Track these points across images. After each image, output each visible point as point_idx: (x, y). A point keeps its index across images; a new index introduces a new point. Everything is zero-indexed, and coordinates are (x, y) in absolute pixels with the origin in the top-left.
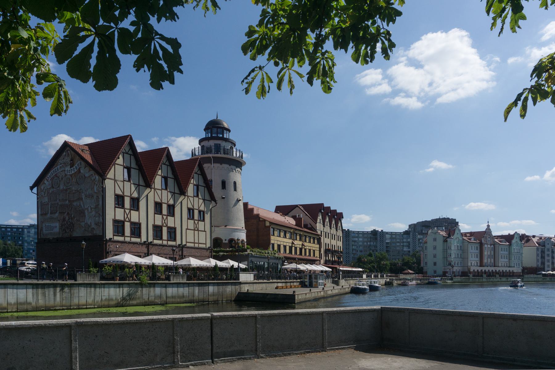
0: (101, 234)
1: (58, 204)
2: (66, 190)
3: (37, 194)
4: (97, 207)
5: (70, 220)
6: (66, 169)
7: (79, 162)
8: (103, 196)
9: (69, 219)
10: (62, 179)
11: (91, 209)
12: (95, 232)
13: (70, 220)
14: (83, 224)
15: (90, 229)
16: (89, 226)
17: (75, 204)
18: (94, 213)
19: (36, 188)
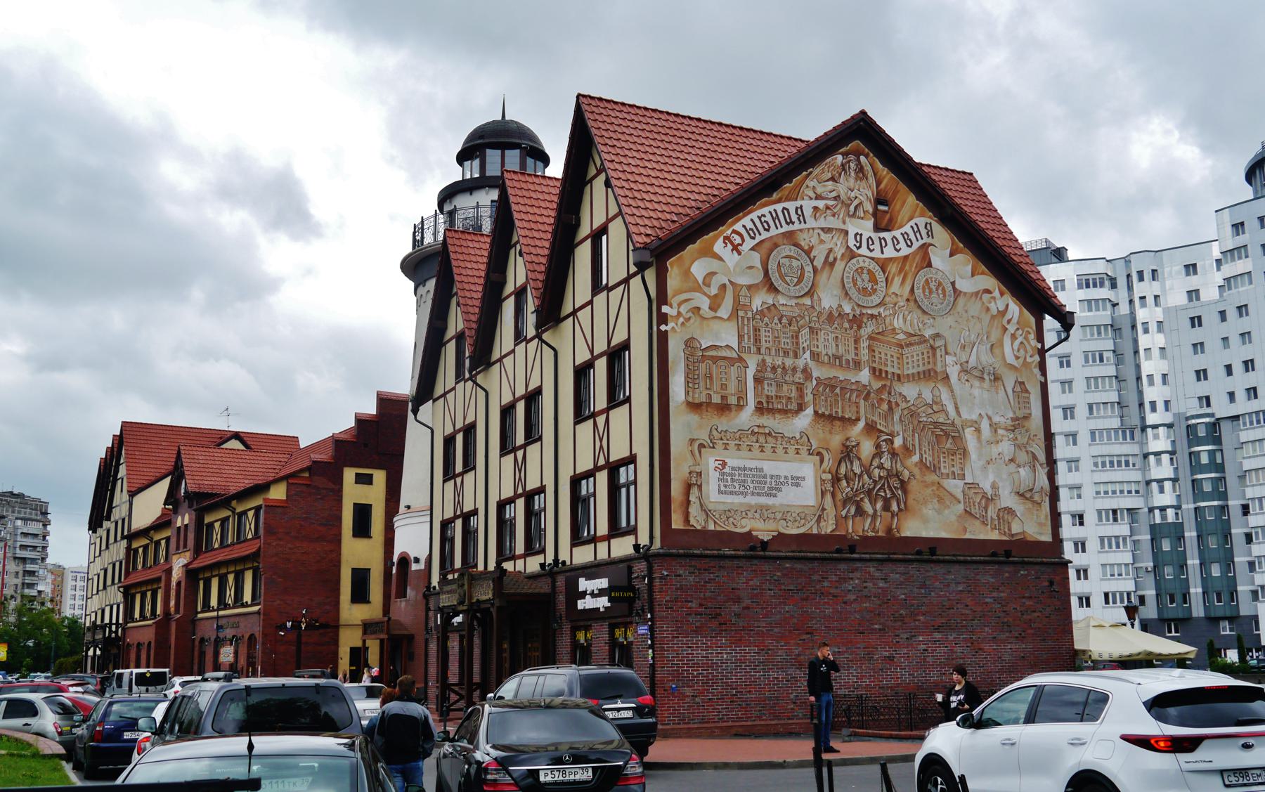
0: (1047, 537)
1: (806, 371)
2: (857, 321)
4: (1019, 423)
9: (878, 454)
10: (830, 264)
11: (994, 427)
12: (1016, 528)
13: (886, 461)
14: (955, 486)
15: (992, 512)
16: (989, 500)
17: (909, 391)
18: (1006, 448)
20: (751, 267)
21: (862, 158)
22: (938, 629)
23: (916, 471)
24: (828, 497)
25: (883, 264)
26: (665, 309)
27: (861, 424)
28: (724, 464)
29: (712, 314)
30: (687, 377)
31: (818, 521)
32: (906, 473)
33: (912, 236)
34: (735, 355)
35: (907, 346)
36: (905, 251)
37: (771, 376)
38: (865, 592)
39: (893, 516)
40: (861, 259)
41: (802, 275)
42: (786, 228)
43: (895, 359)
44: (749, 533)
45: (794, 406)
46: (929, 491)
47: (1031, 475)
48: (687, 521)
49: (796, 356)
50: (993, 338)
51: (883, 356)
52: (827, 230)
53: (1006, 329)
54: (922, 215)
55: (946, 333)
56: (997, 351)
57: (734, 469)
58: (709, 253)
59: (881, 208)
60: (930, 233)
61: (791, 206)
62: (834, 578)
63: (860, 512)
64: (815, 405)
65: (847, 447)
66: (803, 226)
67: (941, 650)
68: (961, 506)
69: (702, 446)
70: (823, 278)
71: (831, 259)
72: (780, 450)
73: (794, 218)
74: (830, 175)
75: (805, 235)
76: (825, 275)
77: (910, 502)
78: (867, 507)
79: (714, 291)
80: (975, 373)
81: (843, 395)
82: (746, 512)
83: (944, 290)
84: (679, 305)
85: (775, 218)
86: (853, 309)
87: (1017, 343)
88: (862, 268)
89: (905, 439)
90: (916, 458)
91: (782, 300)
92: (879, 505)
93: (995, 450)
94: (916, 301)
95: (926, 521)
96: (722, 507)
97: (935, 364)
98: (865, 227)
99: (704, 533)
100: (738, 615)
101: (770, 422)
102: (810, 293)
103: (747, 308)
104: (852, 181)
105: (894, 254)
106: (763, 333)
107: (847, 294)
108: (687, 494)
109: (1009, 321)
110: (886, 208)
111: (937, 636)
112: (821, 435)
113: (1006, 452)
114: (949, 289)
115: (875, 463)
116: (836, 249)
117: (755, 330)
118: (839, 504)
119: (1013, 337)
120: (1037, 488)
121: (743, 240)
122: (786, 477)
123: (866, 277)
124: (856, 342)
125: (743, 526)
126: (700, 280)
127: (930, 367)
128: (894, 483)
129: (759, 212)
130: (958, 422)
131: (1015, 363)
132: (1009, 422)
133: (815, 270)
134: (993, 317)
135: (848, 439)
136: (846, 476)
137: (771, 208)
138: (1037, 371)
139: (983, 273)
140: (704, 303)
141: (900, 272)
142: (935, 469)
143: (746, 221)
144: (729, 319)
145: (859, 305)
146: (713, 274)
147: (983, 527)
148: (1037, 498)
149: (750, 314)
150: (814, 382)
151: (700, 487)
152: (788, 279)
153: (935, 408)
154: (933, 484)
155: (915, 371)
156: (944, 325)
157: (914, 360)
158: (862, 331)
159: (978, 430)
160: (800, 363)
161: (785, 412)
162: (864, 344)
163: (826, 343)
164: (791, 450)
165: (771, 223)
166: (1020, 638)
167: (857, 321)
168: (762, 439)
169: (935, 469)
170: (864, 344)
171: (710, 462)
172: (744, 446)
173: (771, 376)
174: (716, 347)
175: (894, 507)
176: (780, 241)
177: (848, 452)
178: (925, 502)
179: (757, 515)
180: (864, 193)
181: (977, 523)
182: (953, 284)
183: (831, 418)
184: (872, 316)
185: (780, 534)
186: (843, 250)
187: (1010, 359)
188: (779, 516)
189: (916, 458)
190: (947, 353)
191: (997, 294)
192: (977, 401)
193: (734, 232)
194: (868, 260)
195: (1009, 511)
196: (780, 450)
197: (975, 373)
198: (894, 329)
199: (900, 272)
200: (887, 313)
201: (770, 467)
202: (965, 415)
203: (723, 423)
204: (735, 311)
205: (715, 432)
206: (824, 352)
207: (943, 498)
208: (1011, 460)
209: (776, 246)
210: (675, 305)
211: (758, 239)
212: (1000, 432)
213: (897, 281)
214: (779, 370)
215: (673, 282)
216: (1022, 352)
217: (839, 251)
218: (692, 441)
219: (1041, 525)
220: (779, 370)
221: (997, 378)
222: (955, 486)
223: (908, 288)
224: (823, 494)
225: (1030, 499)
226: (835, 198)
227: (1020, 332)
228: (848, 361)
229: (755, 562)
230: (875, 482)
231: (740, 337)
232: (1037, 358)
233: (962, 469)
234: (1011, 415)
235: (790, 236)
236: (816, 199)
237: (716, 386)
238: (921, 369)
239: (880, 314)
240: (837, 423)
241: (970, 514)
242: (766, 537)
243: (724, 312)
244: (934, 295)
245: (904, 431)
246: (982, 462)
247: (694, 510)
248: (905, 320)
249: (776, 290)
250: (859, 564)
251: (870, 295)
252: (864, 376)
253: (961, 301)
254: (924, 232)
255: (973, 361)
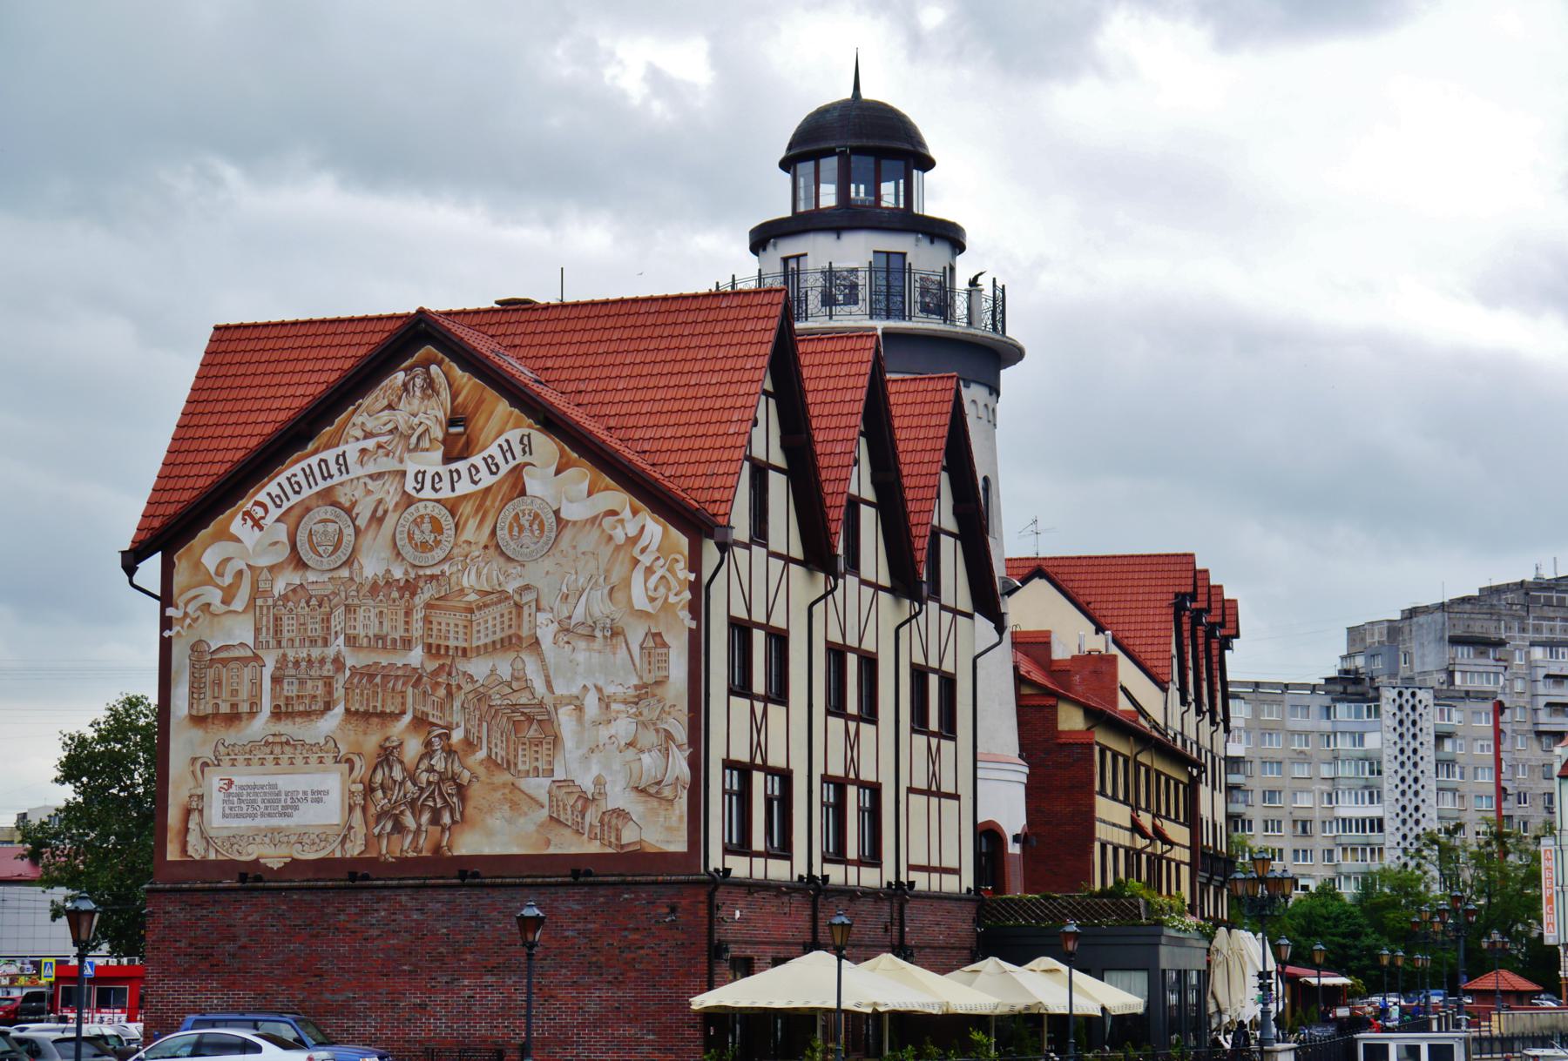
0: (679, 845)
1: (338, 663)
2: (410, 588)
3: (166, 599)
4: (645, 692)
5: (439, 762)
6: (411, 468)
7: (514, 435)
8: (694, 636)
9: (428, 752)
10: (377, 519)
11: (605, 701)
12: (629, 836)
13: (439, 762)
14: (538, 787)
15: (592, 816)
16: (587, 800)
17: (478, 668)
18: (623, 727)
19: (157, 558)
20: (276, 543)
21: (434, 369)
22: (491, 971)
23: (481, 771)
24: (358, 813)
25: (452, 507)
26: (170, 612)
27: (407, 718)
28: (231, 783)
29: (224, 608)
30: (192, 686)
31: (343, 842)
32: (466, 775)
33: (499, 459)
34: (250, 654)
35: (479, 608)
36: (487, 480)
37: (293, 672)
38: (393, 926)
39: (443, 831)
40: (421, 505)
41: (340, 540)
42: (322, 485)
43: (461, 630)
44: (256, 861)
45: (320, 706)
46: (498, 795)
47: (661, 762)
48: (184, 851)
49: (326, 643)
50: (615, 578)
51: (443, 627)
52: (380, 475)
53: (636, 562)
54: (517, 426)
55: (540, 583)
56: (618, 595)
57: (242, 788)
58: (225, 535)
59: (453, 430)
60: (527, 448)
61: (330, 455)
62: (353, 910)
63: (399, 828)
64: (347, 701)
65: (386, 749)
66: (345, 477)
67: (495, 997)
68: (545, 812)
69: (205, 764)
70: (367, 540)
71: (380, 513)
72: (299, 761)
73: (334, 469)
74: (385, 402)
75: (347, 489)
76: (371, 534)
77: (469, 811)
78: (409, 821)
79: (228, 580)
80: (581, 630)
81: (384, 685)
82: (253, 836)
83: (542, 525)
84: (186, 605)
85: (309, 474)
86: (406, 573)
87: (653, 580)
88: (422, 517)
89: (467, 731)
90: (482, 754)
91: (311, 577)
92: (425, 818)
93: (604, 733)
94: (498, 546)
95: (490, 833)
96: (225, 833)
97: (519, 626)
98: (432, 461)
99: (204, 863)
100: (234, 956)
101: (287, 728)
102: (348, 562)
103: (266, 594)
104: (416, 402)
105: (472, 488)
106: (285, 621)
107: (399, 554)
108: (186, 820)
109: (643, 551)
110: (461, 429)
111: (490, 979)
112: (352, 737)
113: (622, 732)
114: (550, 520)
115: (423, 766)
116: (388, 499)
117: (276, 619)
118: (372, 820)
119: (649, 571)
120: (669, 778)
121: (266, 511)
122: (305, 793)
123: (427, 526)
124: (407, 614)
125: (249, 853)
126: (212, 570)
127: (512, 631)
128: (449, 788)
129: (288, 473)
130: (549, 701)
131: (649, 608)
132: (632, 692)
133: (357, 531)
134: (618, 548)
135: (387, 739)
136: (382, 785)
137: (304, 464)
138: (685, 615)
139: (607, 488)
140: (214, 596)
141: (477, 512)
142: (509, 765)
143: (272, 488)
144: (245, 611)
145: (414, 566)
146: (229, 559)
147: (575, 837)
148: (667, 792)
149: (270, 602)
150: (348, 673)
151: (201, 811)
152: (320, 549)
153: (515, 685)
154: (504, 785)
155: (488, 640)
156: (540, 573)
157: (490, 625)
158: (417, 600)
159: (580, 709)
160: (331, 652)
161: (307, 714)
162: (418, 615)
163: (366, 622)
164: (313, 759)
165: (304, 483)
166: (617, 983)
167: (410, 588)
168: (277, 750)
169: (509, 765)
170: (418, 615)
171: (215, 780)
172: (255, 760)
173: (293, 672)
174: (227, 647)
175: (446, 819)
176: (313, 503)
177: (387, 755)
178: (491, 810)
179: (267, 840)
180: (431, 415)
181: (567, 832)
182: (557, 513)
183: (366, 715)
184: (432, 577)
185: (294, 861)
186: (397, 498)
187: (640, 600)
188: (293, 839)
189: (482, 754)
190: (538, 609)
191: (627, 514)
192: (581, 669)
193: (257, 503)
194: (430, 504)
195: (621, 814)
196: (299, 761)
197: (581, 630)
198: (462, 590)
199: (477, 512)
200: (454, 569)
201: (286, 782)
202: (560, 689)
203: (232, 736)
204: (253, 599)
205: (221, 748)
206: (362, 634)
207: (517, 800)
208: (630, 744)
209: (308, 510)
210: (181, 605)
211: (286, 505)
212: (614, 706)
213: (472, 524)
214: (304, 664)
215: (179, 579)
216: (662, 590)
217: (391, 500)
218: (194, 760)
219: (669, 829)
220: (304, 664)
221: (616, 633)
222: (538, 787)
223: (487, 530)
224: (351, 809)
225: (657, 796)
226: (391, 432)
227: (662, 561)
228: (394, 641)
229: (256, 894)
230: (422, 790)
231: (257, 631)
232: (687, 595)
233: (550, 763)
234: (635, 681)
235: (327, 496)
236: (365, 438)
237: (225, 694)
238: (497, 637)
239: (443, 573)
240: (375, 720)
241: (558, 821)
242: (275, 864)
243: (239, 604)
244: (527, 533)
245: (467, 721)
246: (584, 750)
247: (193, 838)
248: (479, 574)
249: (305, 566)
250: (386, 893)
251: (432, 549)
252: (416, 656)
253: (568, 534)
254: (517, 449)
255: (579, 614)
